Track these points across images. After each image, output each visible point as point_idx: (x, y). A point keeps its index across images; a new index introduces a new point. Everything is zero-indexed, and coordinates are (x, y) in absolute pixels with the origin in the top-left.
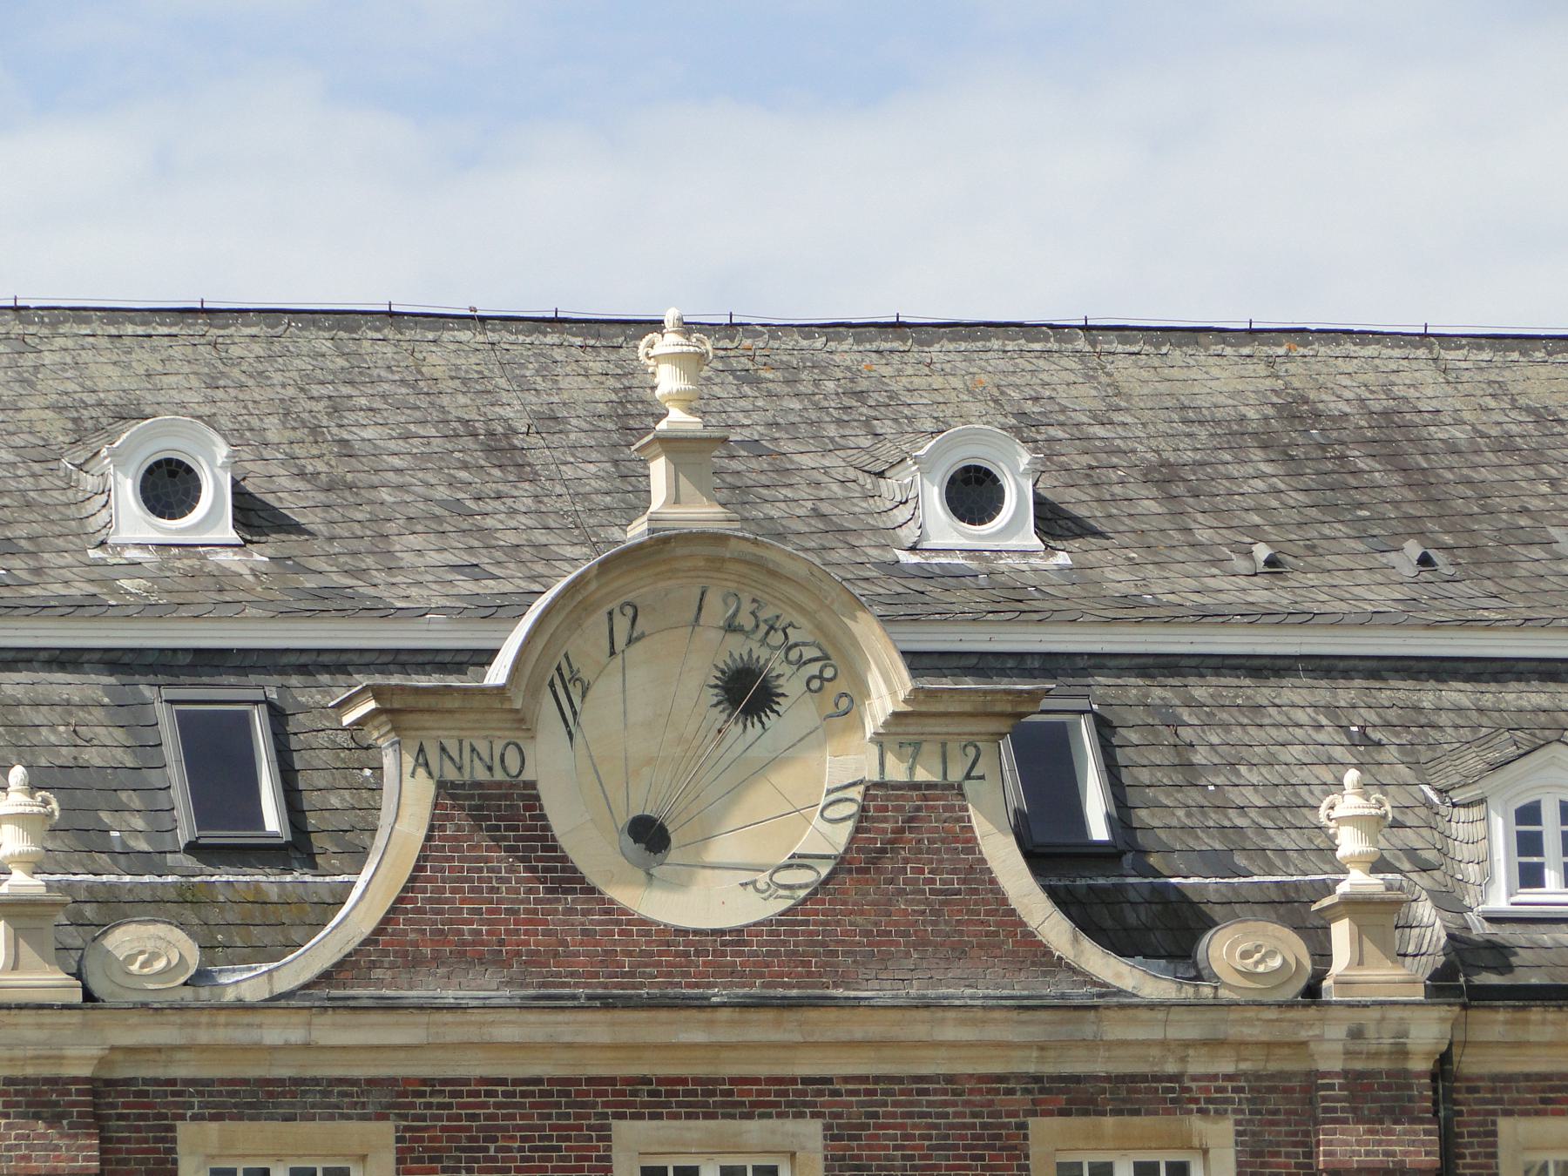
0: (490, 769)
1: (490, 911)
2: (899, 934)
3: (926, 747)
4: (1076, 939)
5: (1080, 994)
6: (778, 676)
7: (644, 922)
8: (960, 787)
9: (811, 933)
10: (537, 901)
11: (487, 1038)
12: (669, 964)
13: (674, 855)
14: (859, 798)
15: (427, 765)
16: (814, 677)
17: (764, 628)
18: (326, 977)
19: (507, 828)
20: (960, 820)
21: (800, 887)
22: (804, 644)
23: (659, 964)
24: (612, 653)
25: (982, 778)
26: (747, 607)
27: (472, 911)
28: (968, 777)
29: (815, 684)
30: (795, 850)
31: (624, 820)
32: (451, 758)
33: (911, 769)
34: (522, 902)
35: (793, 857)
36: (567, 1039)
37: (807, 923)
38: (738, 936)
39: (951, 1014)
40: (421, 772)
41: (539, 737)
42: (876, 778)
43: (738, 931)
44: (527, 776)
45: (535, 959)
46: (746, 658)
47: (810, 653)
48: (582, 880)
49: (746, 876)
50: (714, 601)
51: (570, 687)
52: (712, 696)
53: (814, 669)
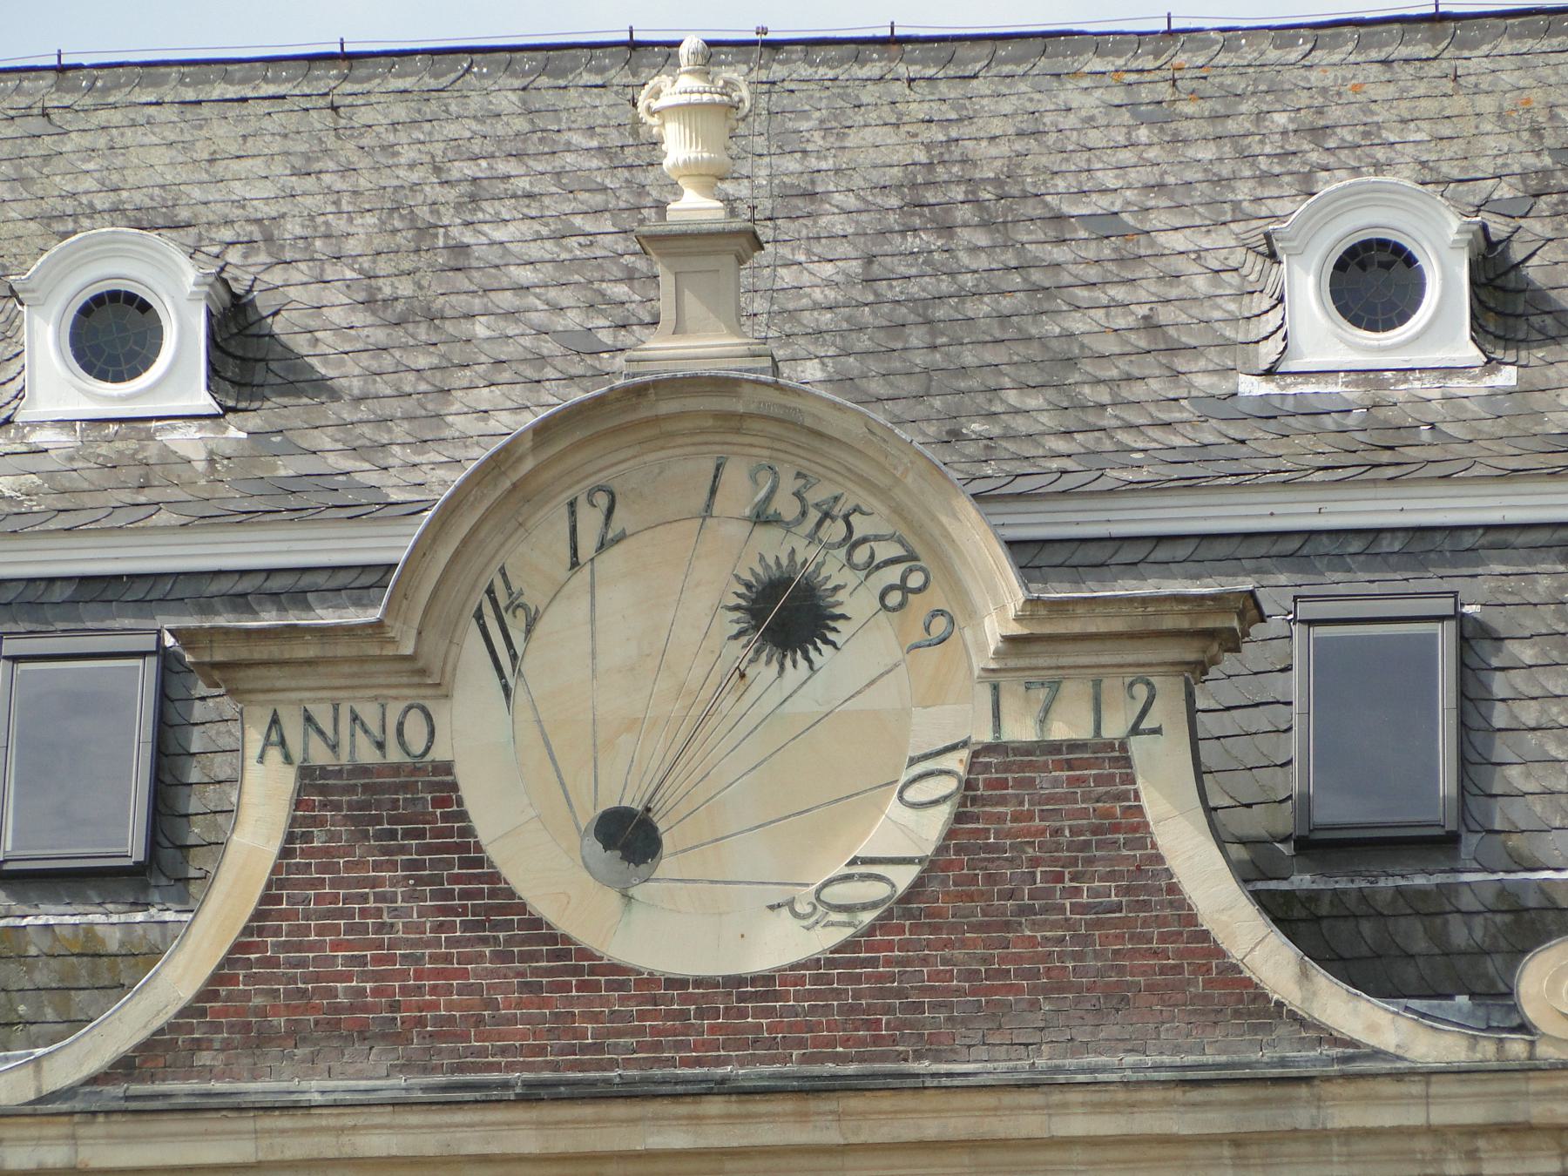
0: (381, 746)
1: (377, 960)
2: (1020, 974)
3: (1068, 688)
4: (1304, 975)
5: (1307, 1057)
6: (836, 589)
8: (1123, 746)
9: (881, 978)
10: (451, 943)
11: (347, 1151)
12: (655, 1031)
13: (667, 865)
14: (961, 770)
15: (282, 743)
16: (892, 588)
17: (814, 515)
18: (125, 1067)
19: (408, 834)
20: (1123, 796)
21: (865, 907)
22: (877, 538)
23: (640, 1031)
24: (575, 564)
25: (1157, 731)
26: (788, 484)
27: (350, 961)
28: (1135, 730)
29: (894, 598)
30: (860, 852)
31: (589, 815)
32: (321, 733)
33: (1043, 722)
34: (427, 944)
35: (853, 862)
36: (473, 1148)
37: (873, 962)
38: (764, 986)
39: (1074, 1096)
40: (275, 754)
41: (458, 695)
42: (988, 737)
43: (767, 979)
44: (439, 753)
45: (447, 1030)
46: (785, 562)
47: (885, 551)
48: (522, 908)
50: (736, 477)
51: (508, 618)
52: (730, 623)
53: (893, 575)
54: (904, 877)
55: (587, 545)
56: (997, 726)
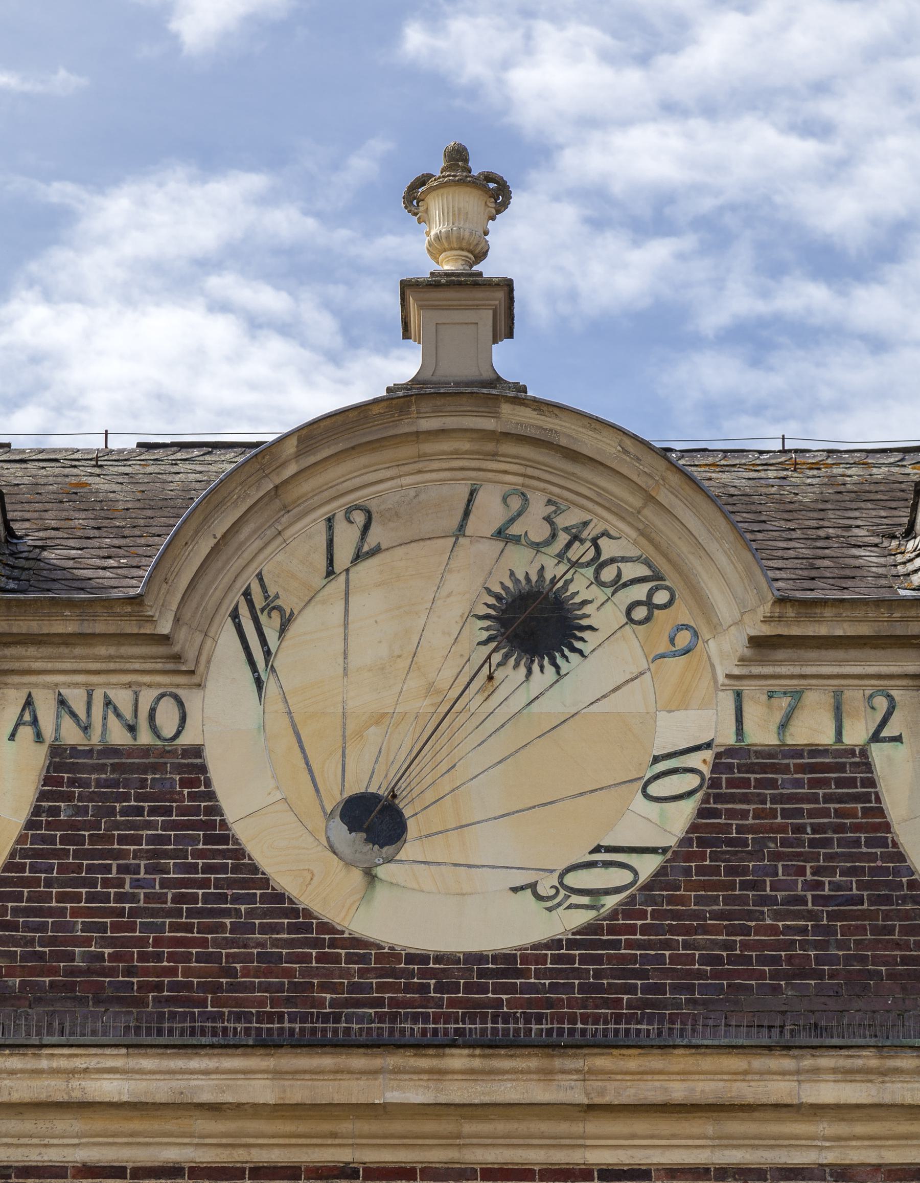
0: (132, 729)
1: (116, 927)
2: (762, 960)
3: (811, 697)
6: (585, 603)
7: (357, 942)
8: (864, 753)
9: (623, 959)
10: (191, 913)
11: (77, 1096)
12: (394, 1003)
13: (410, 850)
14: (706, 770)
15: (35, 722)
16: (638, 603)
17: (563, 538)
19: (153, 811)
20: (865, 798)
21: (607, 892)
22: (624, 559)
23: (379, 1003)
24: (330, 572)
25: (898, 739)
26: (538, 508)
27: (86, 927)
28: (876, 737)
29: (640, 613)
31: (334, 797)
32: (73, 715)
33: (783, 726)
34: (169, 913)
35: (597, 849)
36: (206, 1097)
37: (615, 945)
38: (506, 965)
40: (26, 732)
41: (210, 685)
42: (728, 738)
43: (506, 958)
46: (534, 578)
47: (630, 571)
48: (265, 882)
49: (521, 879)
51: (263, 618)
52: (478, 631)
53: (640, 592)
54: (647, 866)
55: (343, 557)
56: (740, 731)
